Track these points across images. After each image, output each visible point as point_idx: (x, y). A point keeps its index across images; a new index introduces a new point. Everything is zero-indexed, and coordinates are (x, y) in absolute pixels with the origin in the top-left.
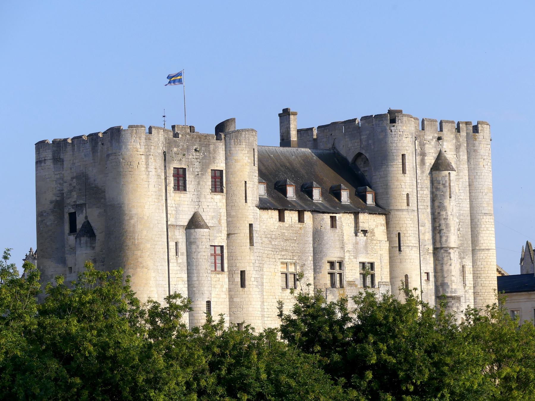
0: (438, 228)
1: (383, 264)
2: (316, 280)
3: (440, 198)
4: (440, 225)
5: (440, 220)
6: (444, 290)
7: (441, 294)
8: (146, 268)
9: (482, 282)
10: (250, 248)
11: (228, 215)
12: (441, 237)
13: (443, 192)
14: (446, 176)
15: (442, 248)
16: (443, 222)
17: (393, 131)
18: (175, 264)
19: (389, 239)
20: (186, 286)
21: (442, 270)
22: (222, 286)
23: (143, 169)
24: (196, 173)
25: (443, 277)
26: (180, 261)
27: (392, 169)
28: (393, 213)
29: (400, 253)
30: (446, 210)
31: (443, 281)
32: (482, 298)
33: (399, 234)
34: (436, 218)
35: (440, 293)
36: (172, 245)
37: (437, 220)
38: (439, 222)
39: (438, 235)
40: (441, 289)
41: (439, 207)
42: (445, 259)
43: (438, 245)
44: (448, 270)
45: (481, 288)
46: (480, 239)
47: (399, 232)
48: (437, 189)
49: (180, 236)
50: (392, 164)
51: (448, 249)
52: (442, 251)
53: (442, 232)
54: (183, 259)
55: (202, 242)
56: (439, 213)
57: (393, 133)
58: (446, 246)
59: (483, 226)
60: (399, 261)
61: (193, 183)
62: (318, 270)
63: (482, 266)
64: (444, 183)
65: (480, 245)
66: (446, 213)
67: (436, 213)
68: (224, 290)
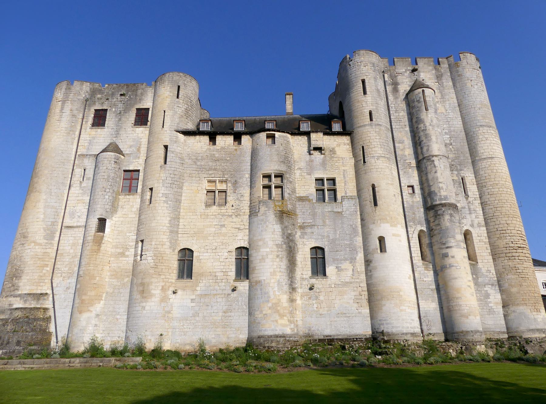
0: (418, 142)
1: (347, 179)
2: (252, 196)
3: (416, 114)
4: (419, 138)
5: (419, 133)
6: (432, 199)
7: (429, 204)
8: (38, 192)
9: (489, 190)
10: (161, 167)
11: (149, 142)
12: (422, 148)
13: (418, 107)
14: (419, 93)
15: (424, 158)
16: (422, 134)
17: (351, 64)
18: (78, 188)
19: (355, 155)
20: (87, 207)
21: (427, 180)
22: (132, 206)
23: (58, 111)
24: (119, 112)
25: (429, 186)
26: (84, 184)
27: (353, 94)
28: (355, 131)
29: (364, 165)
30: (423, 122)
31: (429, 190)
32: (492, 207)
33: (363, 147)
34: (415, 134)
35: (428, 204)
36: (78, 171)
37: (416, 135)
38: (418, 135)
39: (419, 148)
40: (429, 200)
41: (416, 122)
42: (429, 168)
43: (421, 157)
44: (433, 178)
45: (489, 196)
46: (479, 149)
47: (362, 145)
48: (413, 107)
49: (89, 164)
50: (352, 90)
51: (431, 157)
52: (425, 161)
53: (422, 143)
54: (88, 184)
55: (103, 164)
56: (417, 127)
57: (352, 66)
58: (428, 155)
59: (481, 137)
60: (364, 172)
61: (113, 120)
62: (253, 186)
63: (486, 175)
64: (418, 99)
65: (480, 155)
66: (424, 125)
67: (415, 129)
68: (134, 209)
